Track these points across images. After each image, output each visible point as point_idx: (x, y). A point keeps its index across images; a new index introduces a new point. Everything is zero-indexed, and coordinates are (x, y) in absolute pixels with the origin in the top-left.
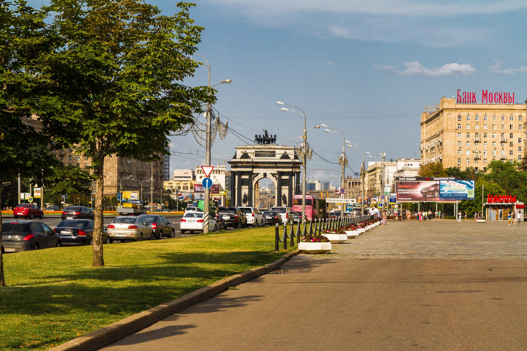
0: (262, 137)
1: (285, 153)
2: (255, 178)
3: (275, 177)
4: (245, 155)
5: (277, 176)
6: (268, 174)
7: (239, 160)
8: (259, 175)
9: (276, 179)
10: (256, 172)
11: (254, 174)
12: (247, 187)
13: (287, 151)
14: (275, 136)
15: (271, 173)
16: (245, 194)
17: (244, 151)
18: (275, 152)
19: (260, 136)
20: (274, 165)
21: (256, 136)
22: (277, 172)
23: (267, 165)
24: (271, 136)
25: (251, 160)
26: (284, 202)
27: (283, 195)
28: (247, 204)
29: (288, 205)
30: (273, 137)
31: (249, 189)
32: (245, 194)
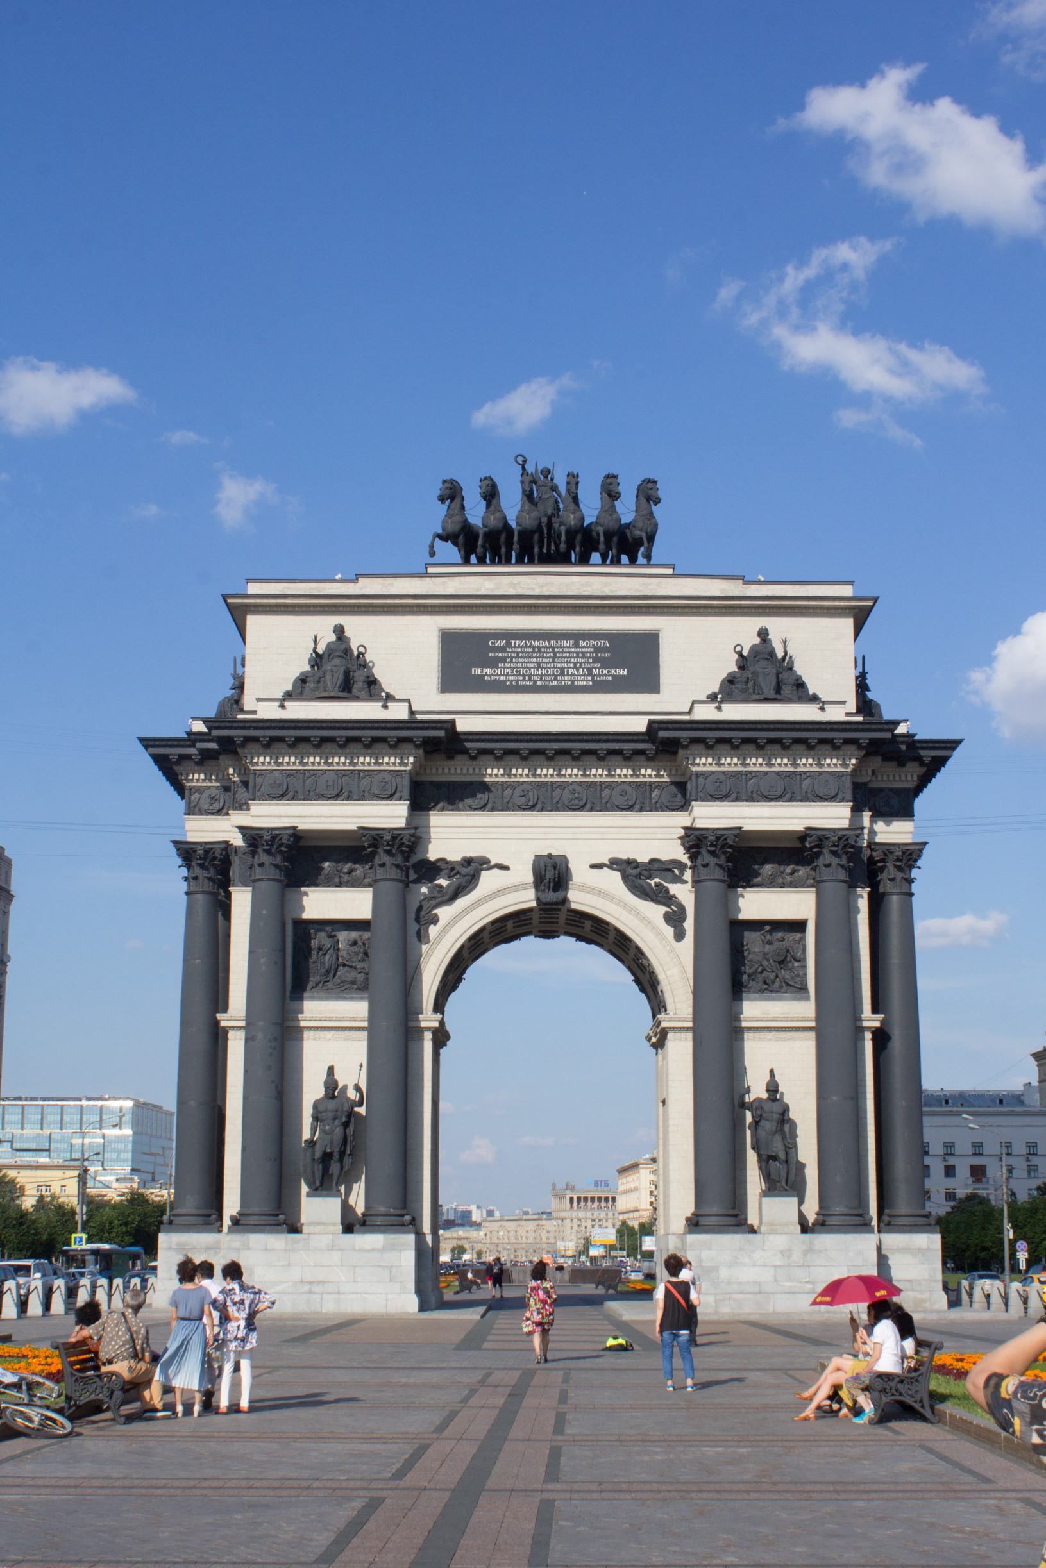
0: (512, 507)
1: (763, 634)
2: (444, 913)
3: (660, 896)
4: (335, 668)
5: (684, 893)
6: (580, 872)
7: (269, 712)
8: (488, 880)
9: (675, 919)
10: (455, 856)
11: (430, 870)
12: (357, 1009)
13: (780, 629)
14: (648, 493)
15: (615, 864)
16: (331, 1085)
17: (323, 628)
18: (651, 640)
19: (491, 494)
20: (648, 774)
21: (452, 493)
22: (695, 840)
23: (572, 774)
24: (610, 491)
25: (398, 712)
26: (767, 1176)
27: (757, 1090)
28: (358, 1199)
29: (811, 1208)
30: (626, 510)
31: (372, 1030)
32: (331, 1085)
